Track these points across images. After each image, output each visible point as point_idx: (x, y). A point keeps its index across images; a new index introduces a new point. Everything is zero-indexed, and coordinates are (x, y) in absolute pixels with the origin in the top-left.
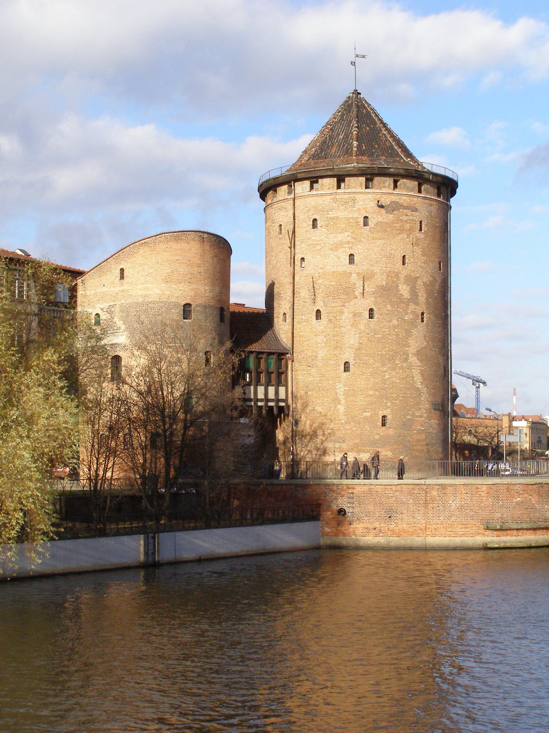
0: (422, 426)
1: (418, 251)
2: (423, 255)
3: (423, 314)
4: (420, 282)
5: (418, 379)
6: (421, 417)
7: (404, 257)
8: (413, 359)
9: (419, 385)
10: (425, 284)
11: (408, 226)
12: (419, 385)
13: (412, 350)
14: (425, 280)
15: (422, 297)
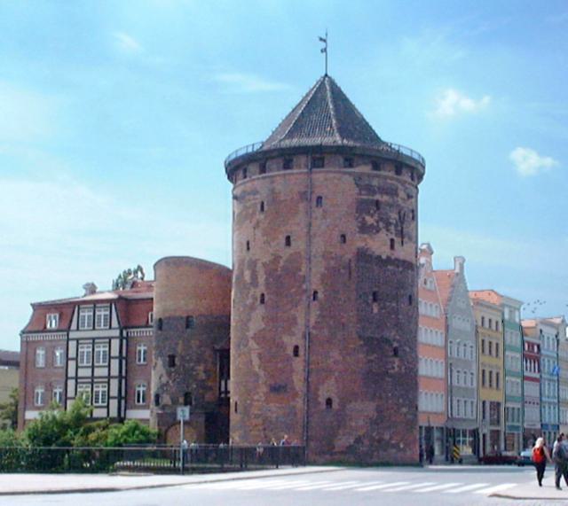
0: (260, 410)
1: (259, 233)
2: (263, 236)
3: (263, 295)
4: (259, 265)
5: (256, 361)
6: (258, 401)
7: (248, 243)
8: (252, 344)
9: (257, 369)
10: (264, 265)
11: (251, 211)
12: (257, 369)
13: (251, 334)
14: (264, 260)
15: (262, 279)
